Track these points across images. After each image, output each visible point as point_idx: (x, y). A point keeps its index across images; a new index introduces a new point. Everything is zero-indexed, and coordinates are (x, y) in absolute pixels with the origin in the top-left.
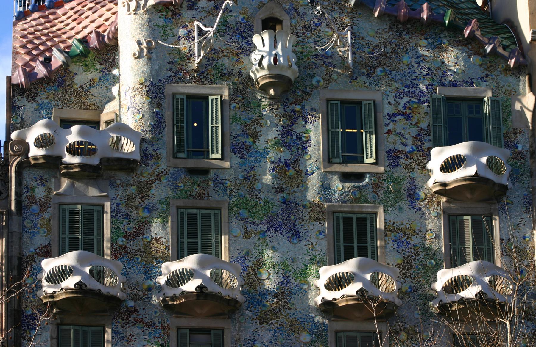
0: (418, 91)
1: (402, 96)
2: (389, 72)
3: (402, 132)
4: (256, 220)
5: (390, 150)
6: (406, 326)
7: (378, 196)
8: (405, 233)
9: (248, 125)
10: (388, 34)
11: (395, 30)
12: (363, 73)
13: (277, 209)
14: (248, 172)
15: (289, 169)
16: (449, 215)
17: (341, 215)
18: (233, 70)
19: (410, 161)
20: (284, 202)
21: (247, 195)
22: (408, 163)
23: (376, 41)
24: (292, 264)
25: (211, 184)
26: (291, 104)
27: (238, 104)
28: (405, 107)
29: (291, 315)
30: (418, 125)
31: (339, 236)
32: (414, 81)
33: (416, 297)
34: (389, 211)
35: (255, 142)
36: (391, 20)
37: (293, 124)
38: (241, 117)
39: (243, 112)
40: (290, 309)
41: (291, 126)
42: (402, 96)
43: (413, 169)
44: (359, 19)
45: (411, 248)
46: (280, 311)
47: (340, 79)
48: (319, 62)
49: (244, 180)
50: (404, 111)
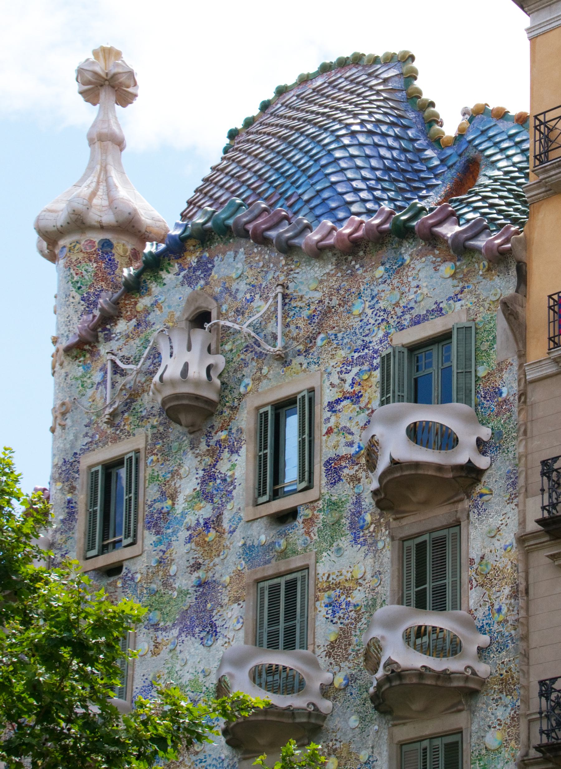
0: (371, 352)
1: (349, 368)
2: (333, 337)
3: (348, 425)
4: (168, 624)
5: (330, 459)
6: (338, 745)
7: (311, 539)
8: (345, 587)
9: (168, 481)
10: (335, 278)
11: (344, 268)
12: (299, 351)
13: (191, 600)
14: (164, 552)
15: (209, 532)
16: (403, 540)
17: (267, 584)
18: (153, 407)
19: (356, 468)
20: (200, 585)
21: (162, 587)
22: (352, 472)
23: (318, 295)
24: (204, 680)
25: (119, 584)
26: (216, 433)
27: (157, 455)
28: (352, 385)
29: (198, 763)
30: (369, 406)
31: (262, 619)
32: (364, 338)
33: (353, 692)
34: (323, 559)
35: (174, 504)
36: (335, 254)
37: (217, 462)
38: (160, 472)
39: (162, 464)
40: (197, 753)
41: (214, 466)
42: (349, 368)
43: (359, 480)
44: (297, 271)
45: (351, 611)
46: (183, 760)
47: (271, 372)
48: (250, 355)
49: (158, 566)
50: (352, 390)
